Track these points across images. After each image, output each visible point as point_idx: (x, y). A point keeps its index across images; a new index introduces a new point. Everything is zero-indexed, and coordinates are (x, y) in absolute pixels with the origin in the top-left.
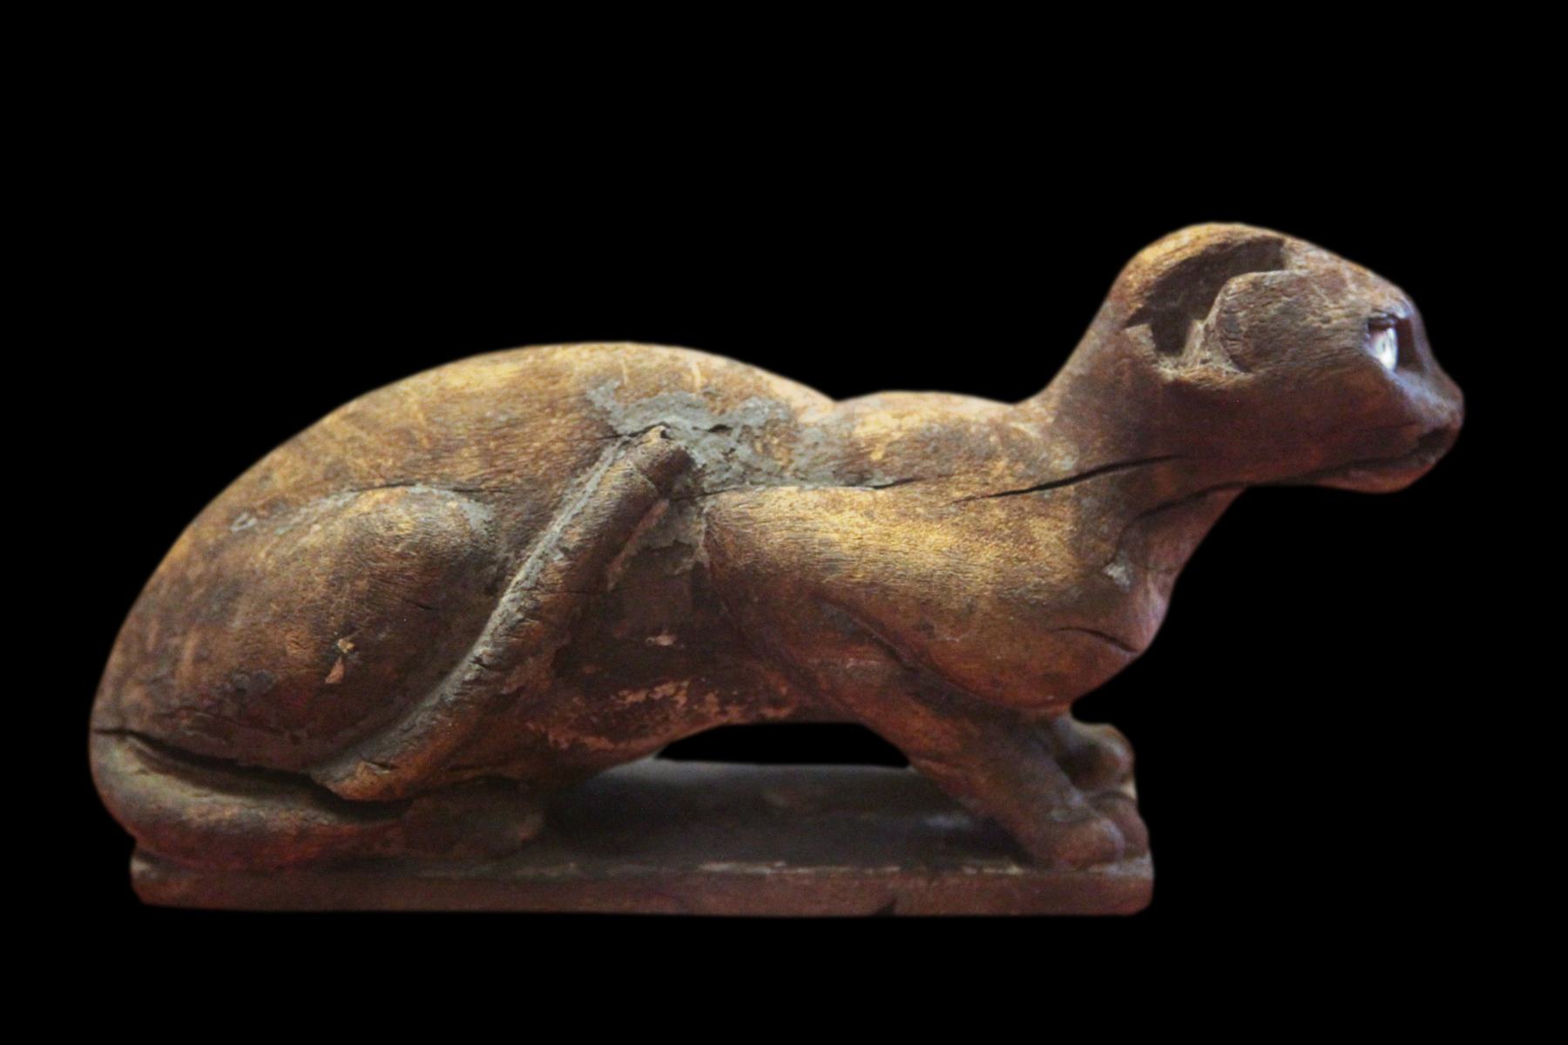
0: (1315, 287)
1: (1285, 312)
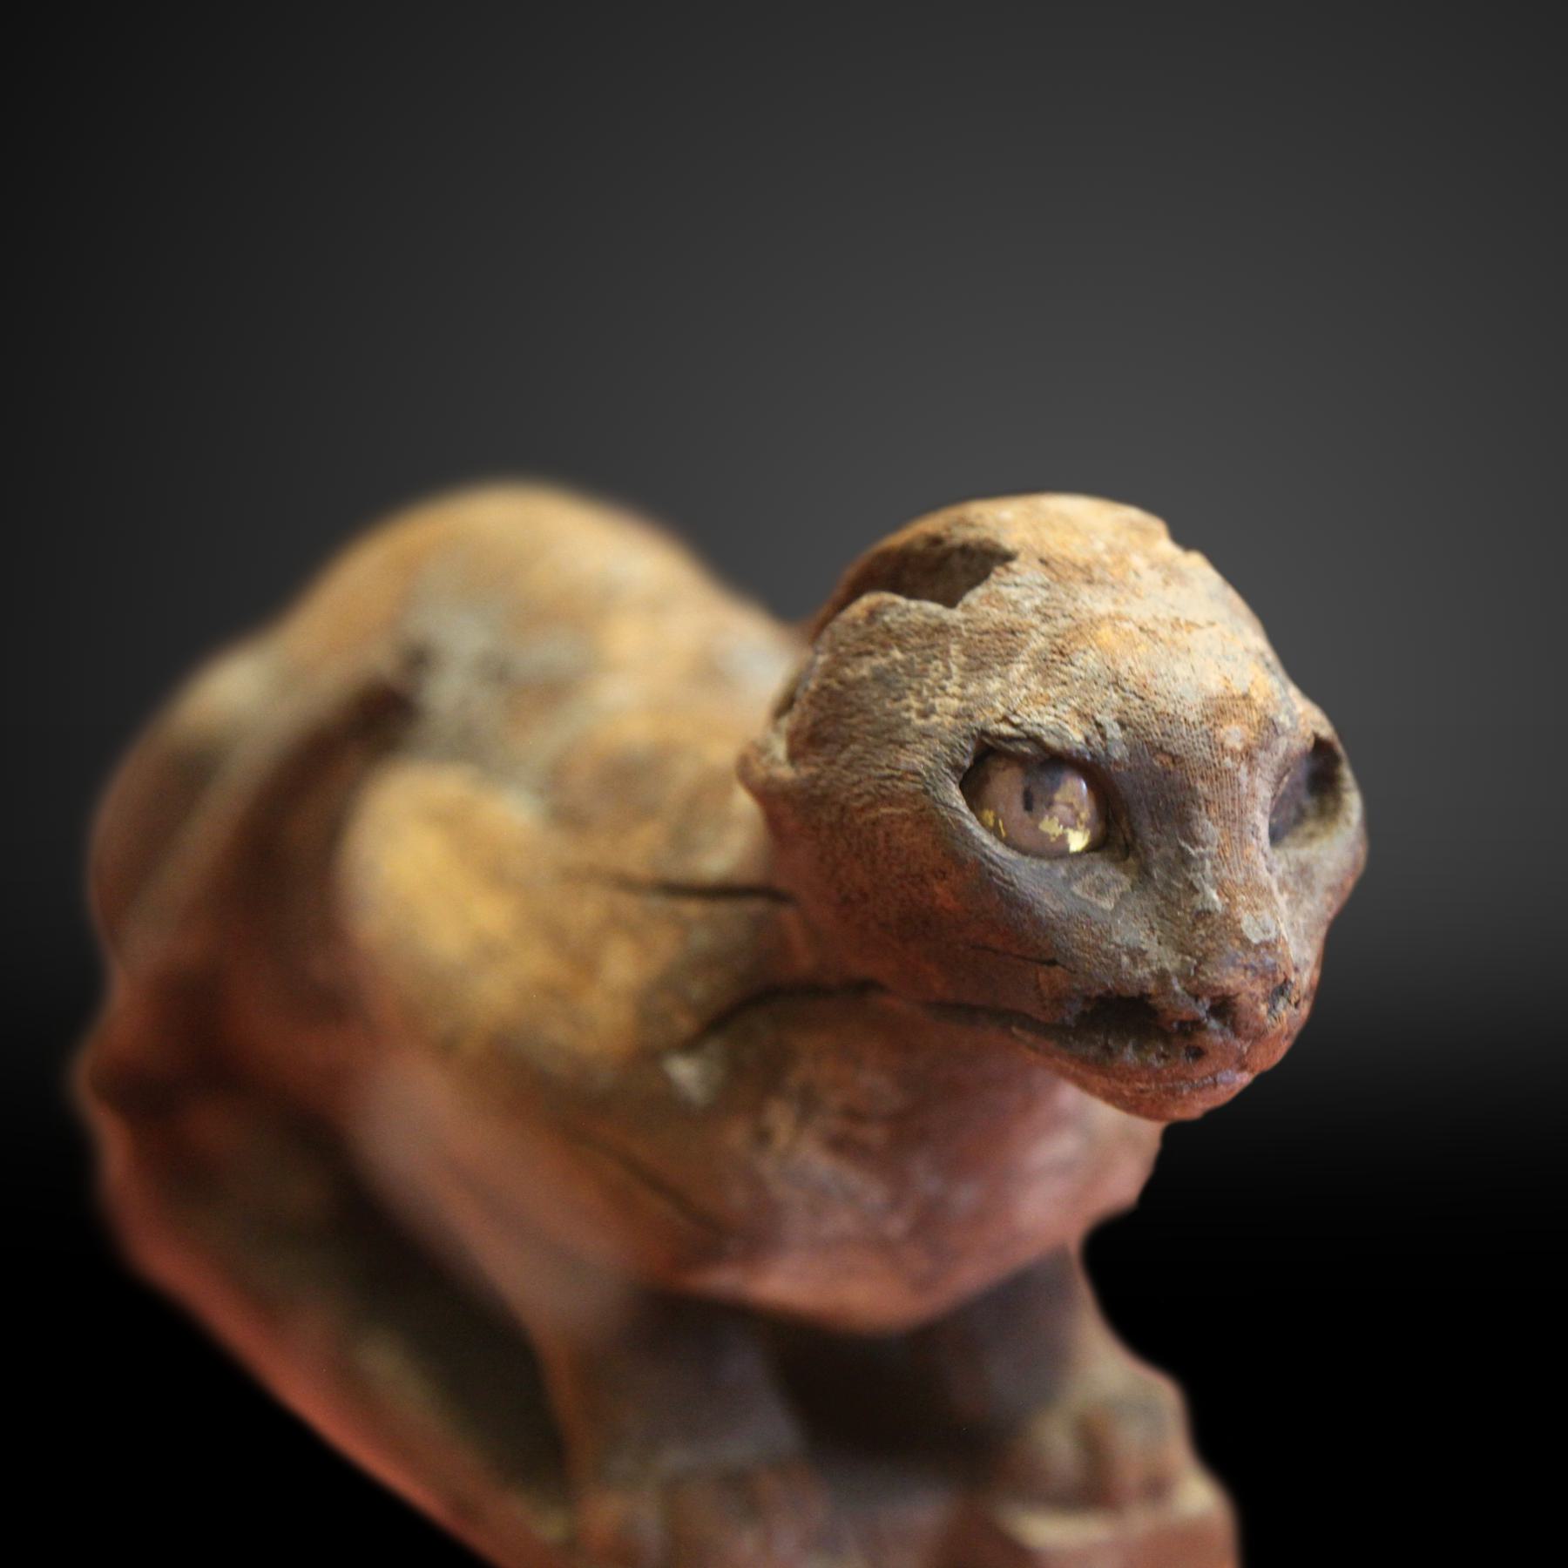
0: (954, 649)
1: (879, 677)
